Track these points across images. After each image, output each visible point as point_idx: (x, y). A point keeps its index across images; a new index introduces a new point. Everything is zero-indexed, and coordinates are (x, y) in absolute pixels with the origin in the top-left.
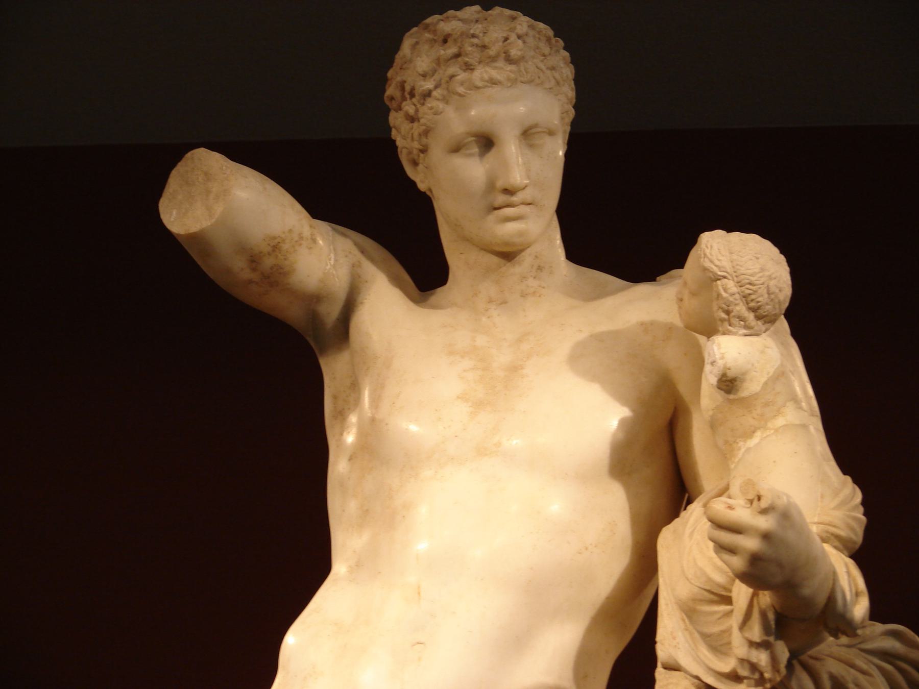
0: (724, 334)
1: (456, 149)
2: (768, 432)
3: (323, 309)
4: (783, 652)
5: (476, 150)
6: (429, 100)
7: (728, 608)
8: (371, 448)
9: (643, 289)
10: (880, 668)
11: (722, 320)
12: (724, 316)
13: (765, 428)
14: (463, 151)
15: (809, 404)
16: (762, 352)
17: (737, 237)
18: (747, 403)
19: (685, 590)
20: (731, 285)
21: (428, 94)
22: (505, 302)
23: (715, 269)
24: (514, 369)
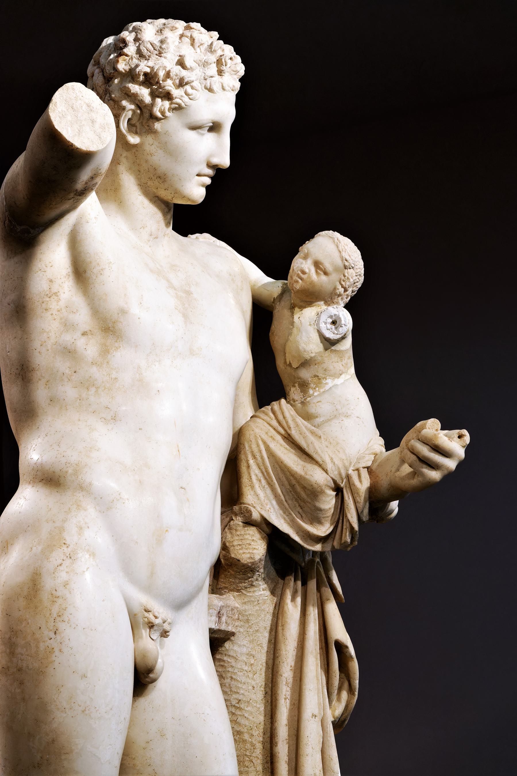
1: (194, 128)
2: (348, 377)
11: (340, 295)
14: (199, 130)
22: (156, 238)
23: (351, 261)
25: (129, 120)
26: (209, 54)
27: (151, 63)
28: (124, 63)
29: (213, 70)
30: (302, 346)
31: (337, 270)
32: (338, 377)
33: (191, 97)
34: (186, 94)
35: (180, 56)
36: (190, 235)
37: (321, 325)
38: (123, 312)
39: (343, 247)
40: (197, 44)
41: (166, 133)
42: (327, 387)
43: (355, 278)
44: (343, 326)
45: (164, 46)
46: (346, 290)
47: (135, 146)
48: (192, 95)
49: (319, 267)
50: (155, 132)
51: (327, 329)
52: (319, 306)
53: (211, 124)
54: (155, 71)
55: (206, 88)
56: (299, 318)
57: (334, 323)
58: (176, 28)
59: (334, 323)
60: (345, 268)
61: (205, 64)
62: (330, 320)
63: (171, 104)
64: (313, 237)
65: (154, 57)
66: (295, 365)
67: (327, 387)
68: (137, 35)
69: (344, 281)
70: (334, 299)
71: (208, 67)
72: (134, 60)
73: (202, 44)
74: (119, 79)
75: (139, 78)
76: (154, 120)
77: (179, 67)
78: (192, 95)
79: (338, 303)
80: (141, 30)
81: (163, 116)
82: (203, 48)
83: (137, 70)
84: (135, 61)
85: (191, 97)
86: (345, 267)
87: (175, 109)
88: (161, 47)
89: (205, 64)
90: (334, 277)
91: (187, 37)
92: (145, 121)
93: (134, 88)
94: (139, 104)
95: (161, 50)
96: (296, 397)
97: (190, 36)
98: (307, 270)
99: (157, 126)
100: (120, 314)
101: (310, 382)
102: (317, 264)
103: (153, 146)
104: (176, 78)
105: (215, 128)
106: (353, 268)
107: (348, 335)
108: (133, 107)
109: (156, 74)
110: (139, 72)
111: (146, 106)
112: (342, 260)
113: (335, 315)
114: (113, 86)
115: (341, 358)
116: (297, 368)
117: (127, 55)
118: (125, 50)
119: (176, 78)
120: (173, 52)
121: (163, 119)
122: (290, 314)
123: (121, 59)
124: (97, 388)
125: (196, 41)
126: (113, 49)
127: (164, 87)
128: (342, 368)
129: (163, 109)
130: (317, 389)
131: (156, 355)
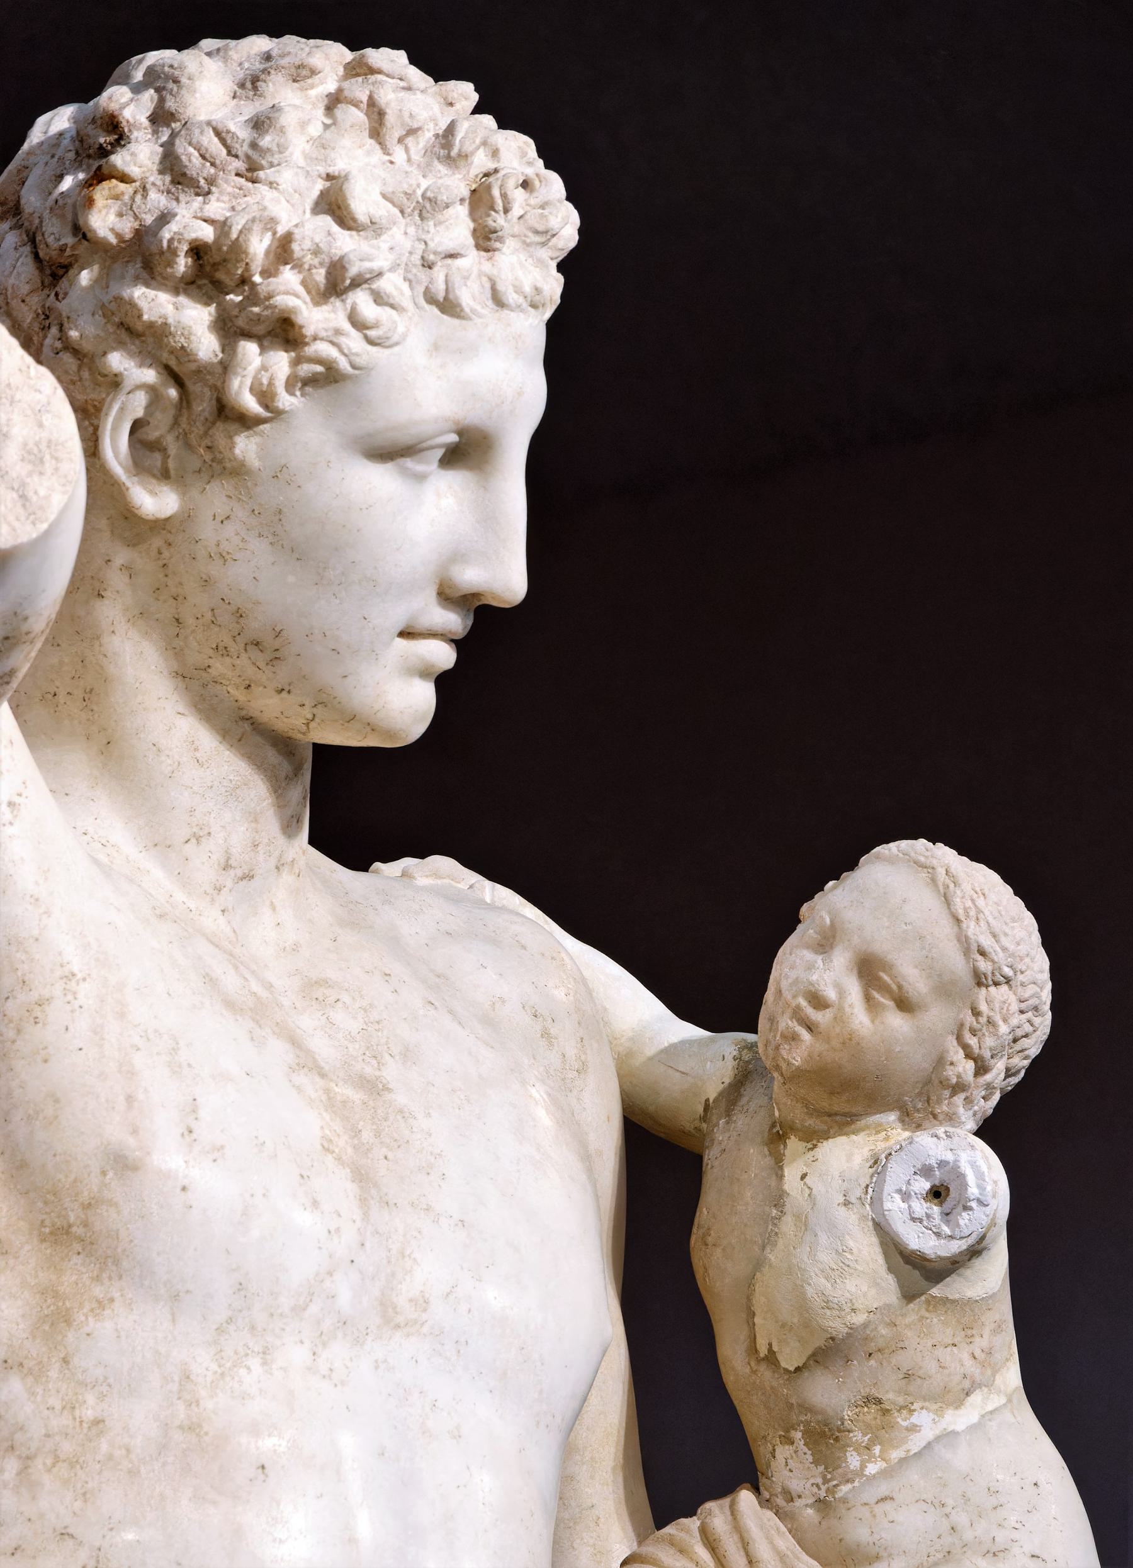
1: (389, 452)
2: (996, 1401)
11: (959, 1087)
13: (989, 1385)
14: (408, 463)
22: (248, 877)
23: (1000, 956)
25: (136, 426)
26: (442, 169)
27: (216, 208)
28: (115, 206)
29: (457, 228)
30: (817, 1285)
31: (945, 989)
32: (958, 1404)
33: (372, 333)
34: (357, 322)
35: (329, 177)
36: (377, 865)
37: (887, 1205)
38: (123, 1164)
39: (969, 904)
40: (393, 133)
41: (280, 473)
42: (916, 1443)
43: (1015, 1021)
44: (974, 1204)
45: (266, 141)
46: (981, 1068)
47: (160, 526)
48: (375, 326)
49: (879, 979)
50: (237, 471)
51: (913, 1219)
52: (879, 1129)
53: (453, 438)
54: (234, 236)
55: (431, 299)
56: (803, 1177)
57: (937, 1194)
58: (313, 72)
59: (937, 1194)
60: (979, 984)
61: (427, 208)
62: (923, 1185)
63: (296, 362)
64: (851, 864)
65: (229, 184)
66: (789, 1359)
67: (916, 1443)
68: (162, 100)
69: (973, 1032)
70: (939, 1101)
71: (439, 216)
72: (153, 195)
73: (412, 132)
74: (96, 268)
75: (171, 263)
76: (233, 427)
77: (327, 221)
78: (375, 326)
79: (951, 1118)
80: (176, 81)
81: (267, 407)
82: (418, 145)
83: (166, 234)
84: (157, 200)
85: (372, 333)
86: (980, 980)
87: (311, 381)
88: (254, 145)
89: (427, 208)
90: (937, 1016)
91: (356, 104)
92: (199, 429)
93: (155, 303)
94: (173, 363)
95: (255, 156)
96: (796, 1485)
97: (365, 99)
98: (831, 994)
99: (245, 446)
100: (111, 1174)
101: (847, 1423)
102: (870, 970)
103: (230, 529)
104: (316, 262)
105: (467, 450)
106: (1008, 981)
107: (995, 1240)
108: (149, 375)
109: (237, 250)
110: (171, 241)
111: (202, 371)
112: (967, 952)
113: (942, 1164)
114: (74, 295)
115: (968, 1330)
116: (798, 1369)
117: (124, 178)
118: (119, 159)
119: (316, 262)
120: (302, 163)
121: (264, 421)
122: (769, 1161)
123: (100, 193)
124: (27, 1460)
125: (390, 118)
126: (72, 155)
127: (270, 297)
128: (970, 1367)
129: (265, 381)
130: (877, 1450)
131: (253, 1328)
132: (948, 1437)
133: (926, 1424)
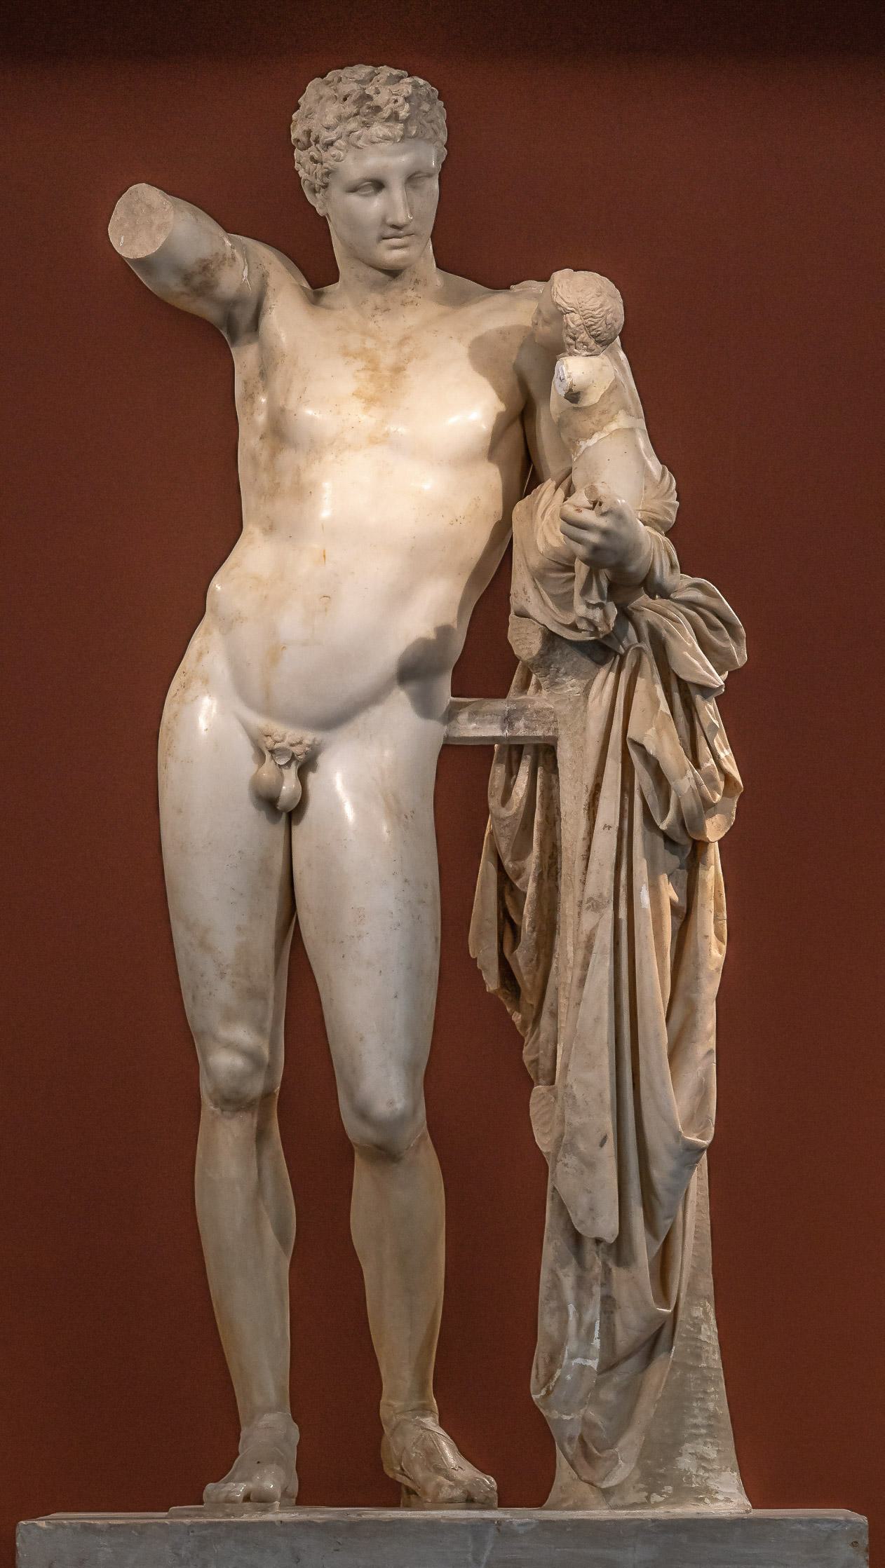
0: (570, 355)
1: (354, 190)
2: (603, 435)
3: (237, 311)
4: (613, 611)
5: (372, 191)
6: (331, 148)
7: (571, 574)
8: (279, 432)
9: (501, 298)
10: (685, 614)
11: (570, 345)
12: (571, 341)
13: (601, 430)
15: (636, 410)
16: (601, 370)
17: (582, 276)
18: (587, 411)
19: (535, 561)
20: (577, 317)
21: (331, 144)
24: (398, 370)
87: (327, 174)
128: (592, 426)
132: (588, 448)
133: (583, 445)
